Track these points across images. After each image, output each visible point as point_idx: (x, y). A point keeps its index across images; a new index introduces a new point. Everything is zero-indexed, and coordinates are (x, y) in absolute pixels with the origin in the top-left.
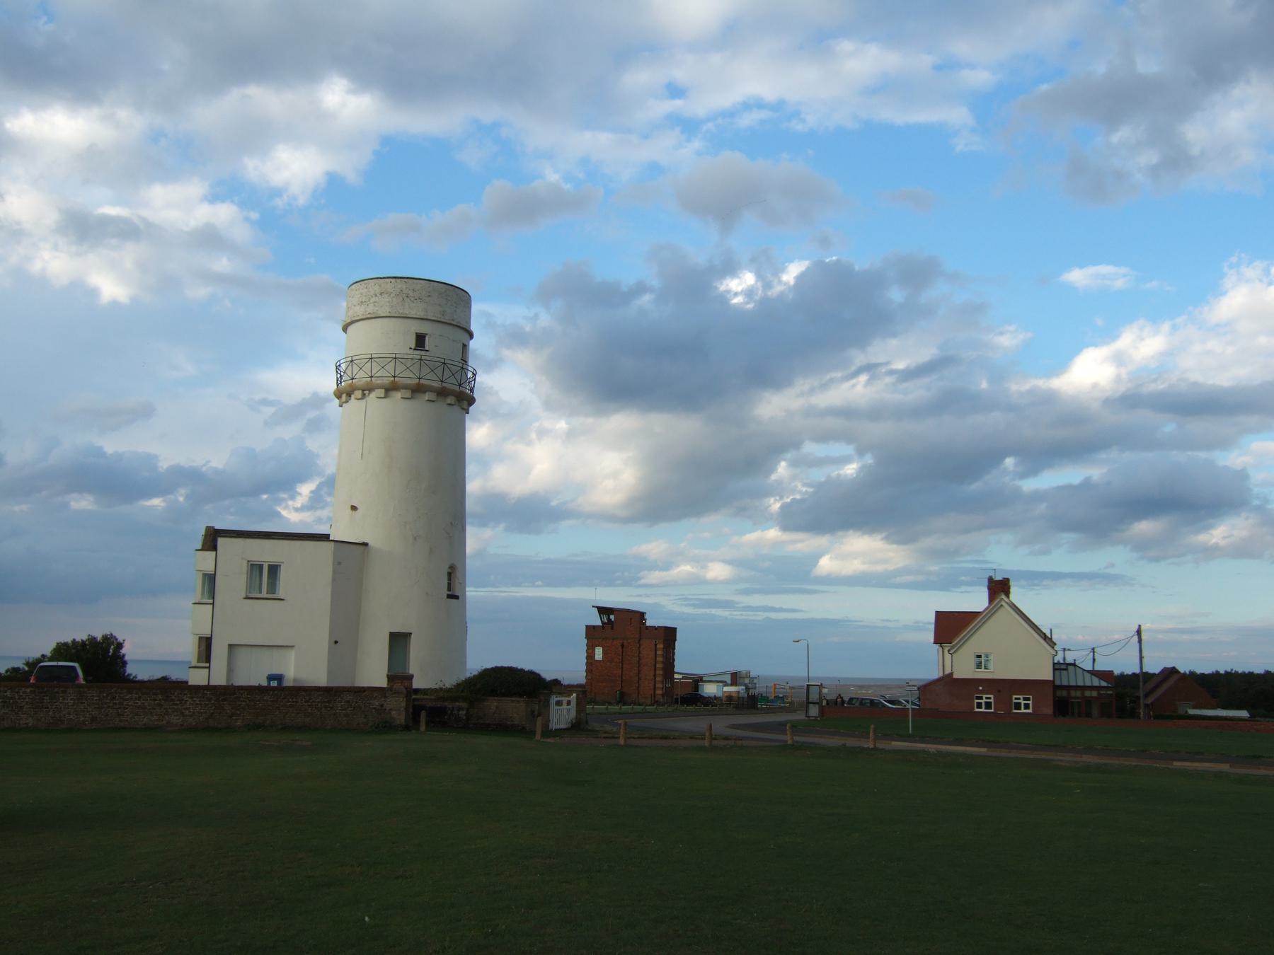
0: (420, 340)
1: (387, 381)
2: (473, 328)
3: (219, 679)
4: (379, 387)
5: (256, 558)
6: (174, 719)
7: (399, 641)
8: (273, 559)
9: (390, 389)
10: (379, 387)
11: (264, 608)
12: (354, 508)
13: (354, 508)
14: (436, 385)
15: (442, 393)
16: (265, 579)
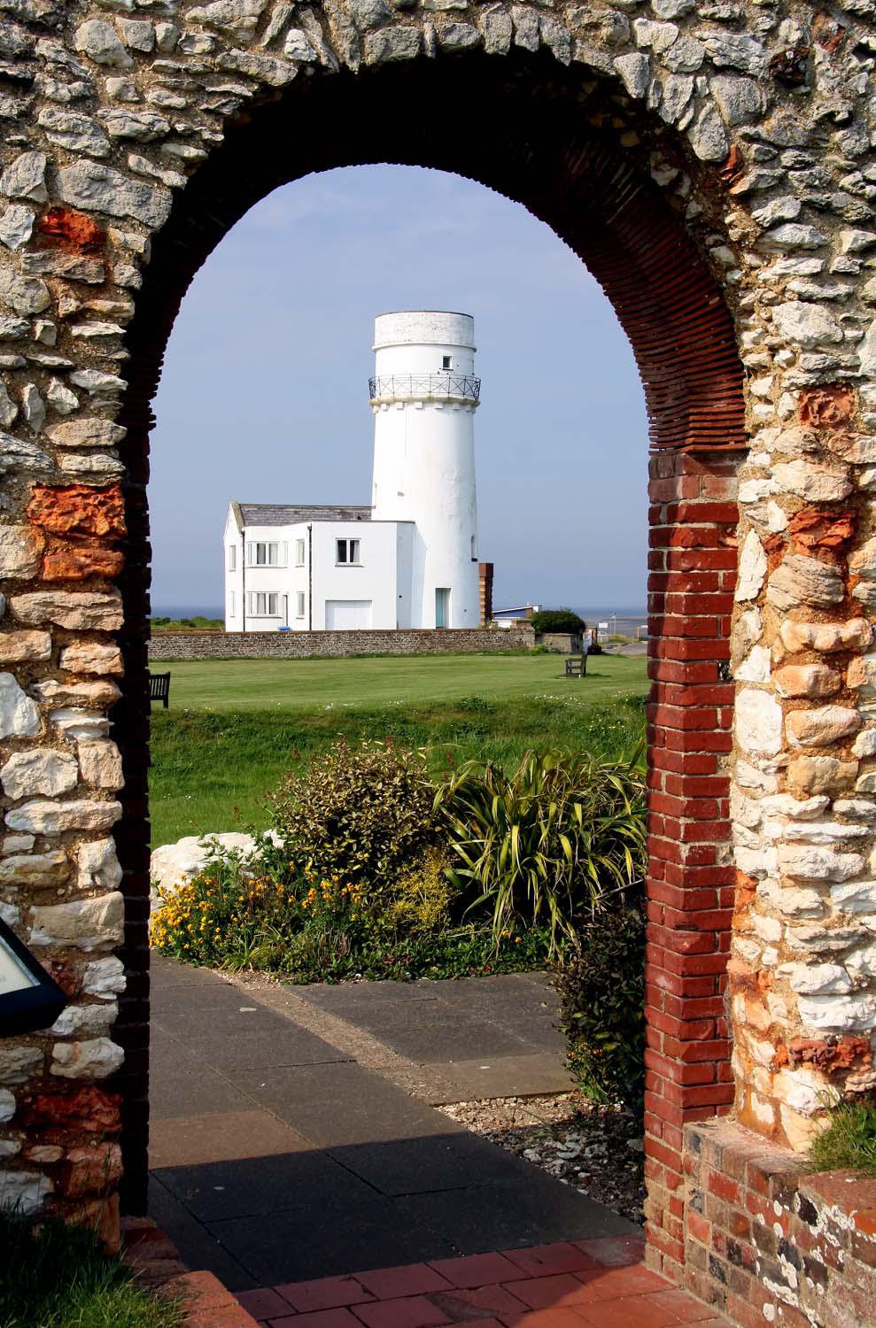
0: (446, 360)
1: (426, 395)
2: (476, 345)
3: (319, 626)
4: (418, 400)
5: (342, 537)
6: (396, 651)
7: (442, 593)
8: (353, 536)
9: (430, 401)
10: (418, 400)
11: (346, 572)
12: (401, 494)
13: (401, 494)
14: (462, 398)
15: (464, 403)
16: (345, 551)
